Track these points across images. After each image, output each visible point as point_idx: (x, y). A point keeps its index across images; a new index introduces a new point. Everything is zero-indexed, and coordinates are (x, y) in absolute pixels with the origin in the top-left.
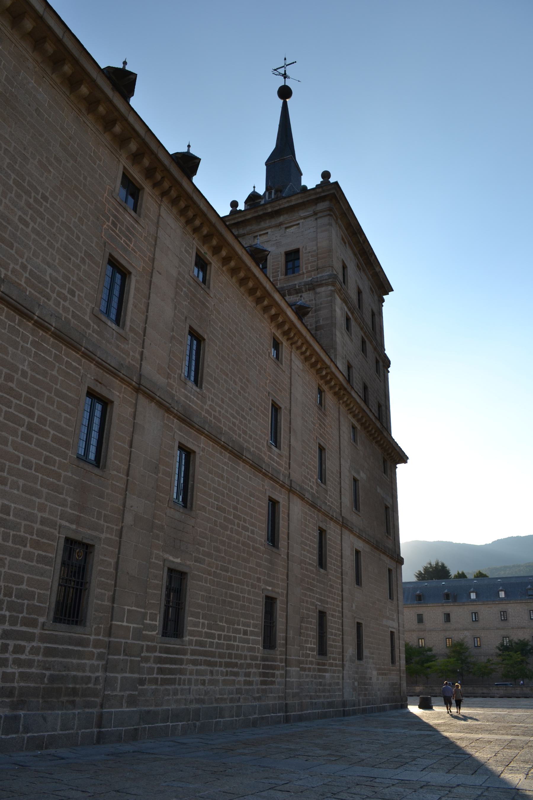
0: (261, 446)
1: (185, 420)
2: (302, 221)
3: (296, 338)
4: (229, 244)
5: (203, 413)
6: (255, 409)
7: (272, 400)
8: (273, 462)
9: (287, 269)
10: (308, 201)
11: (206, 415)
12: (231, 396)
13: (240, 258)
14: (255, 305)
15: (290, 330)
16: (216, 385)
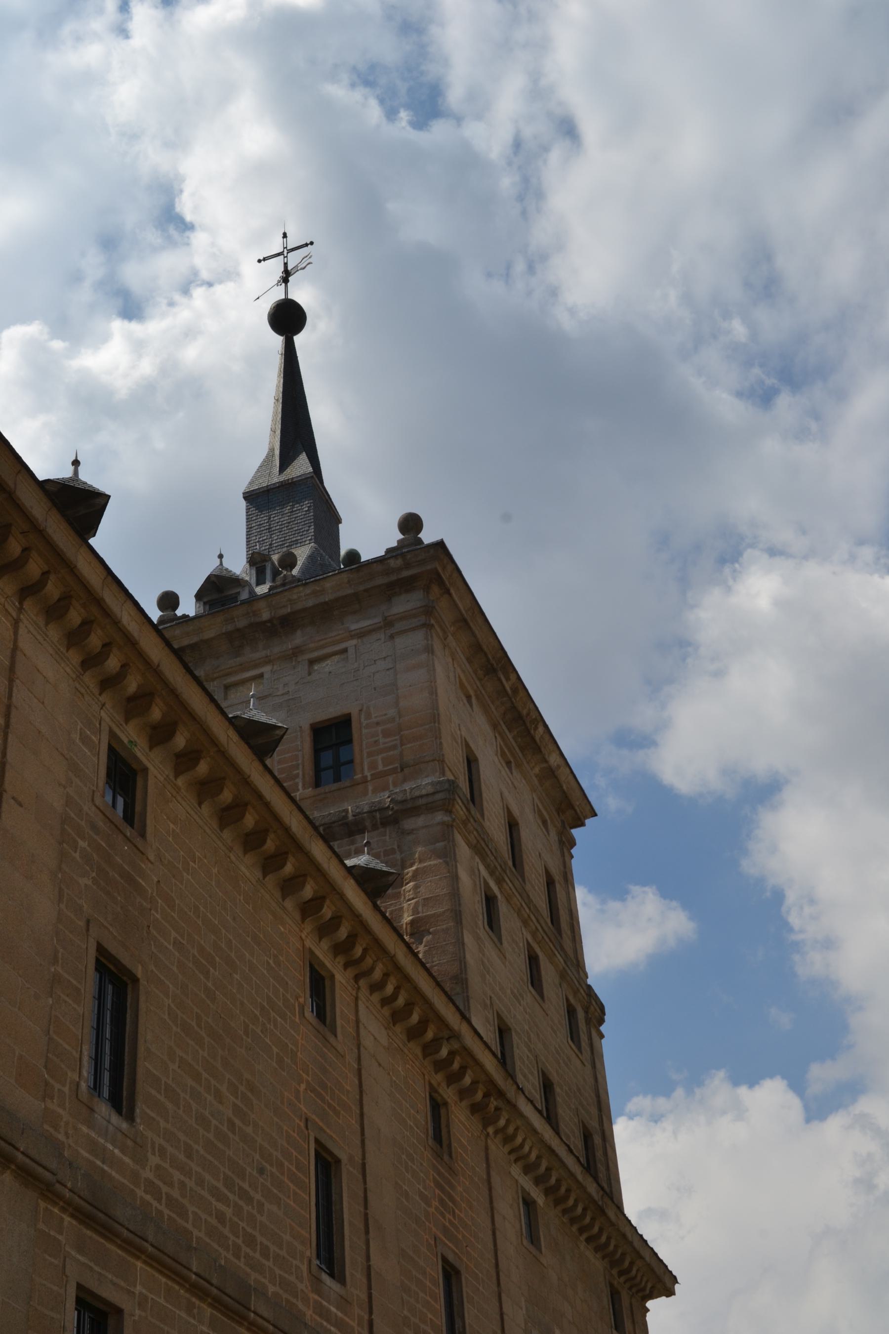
0: (292, 1278)
1: (95, 1215)
3: (369, 961)
4: (193, 716)
5: (140, 1193)
6: (274, 1170)
7: (317, 1141)
8: (328, 1321)
9: (318, 770)
10: (366, 591)
11: (148, 1197)
12: (211, 1136)
13: (223, 753)
14: (259, 874)
15: (352, 938)
16: (170, 1106)
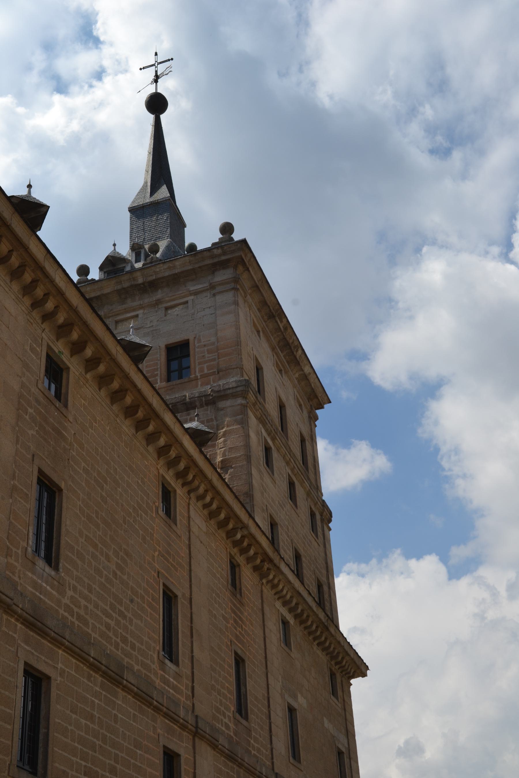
0: (149, 662)
1: (35, 623)
2: (192, 297)
3: (196, 483)
4: (96, 338)
5: (61, 611)
6: (139, 600)
7: (164, 585)
8: (169, 686)
9: (169, 371)
10: (200, 267)
11: (66, 614)
12: (103, 580)
13: (113, 360)
14: (134, 431)
15: (187, 469)
16: (79, 562)
